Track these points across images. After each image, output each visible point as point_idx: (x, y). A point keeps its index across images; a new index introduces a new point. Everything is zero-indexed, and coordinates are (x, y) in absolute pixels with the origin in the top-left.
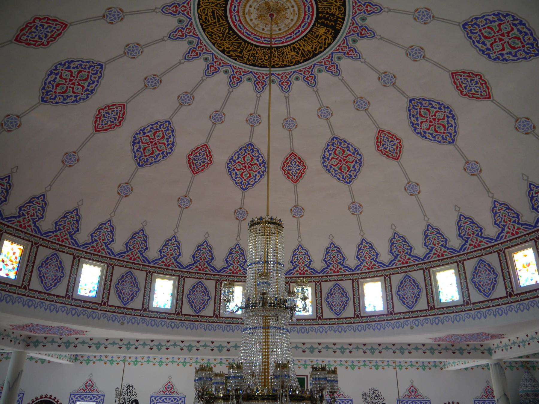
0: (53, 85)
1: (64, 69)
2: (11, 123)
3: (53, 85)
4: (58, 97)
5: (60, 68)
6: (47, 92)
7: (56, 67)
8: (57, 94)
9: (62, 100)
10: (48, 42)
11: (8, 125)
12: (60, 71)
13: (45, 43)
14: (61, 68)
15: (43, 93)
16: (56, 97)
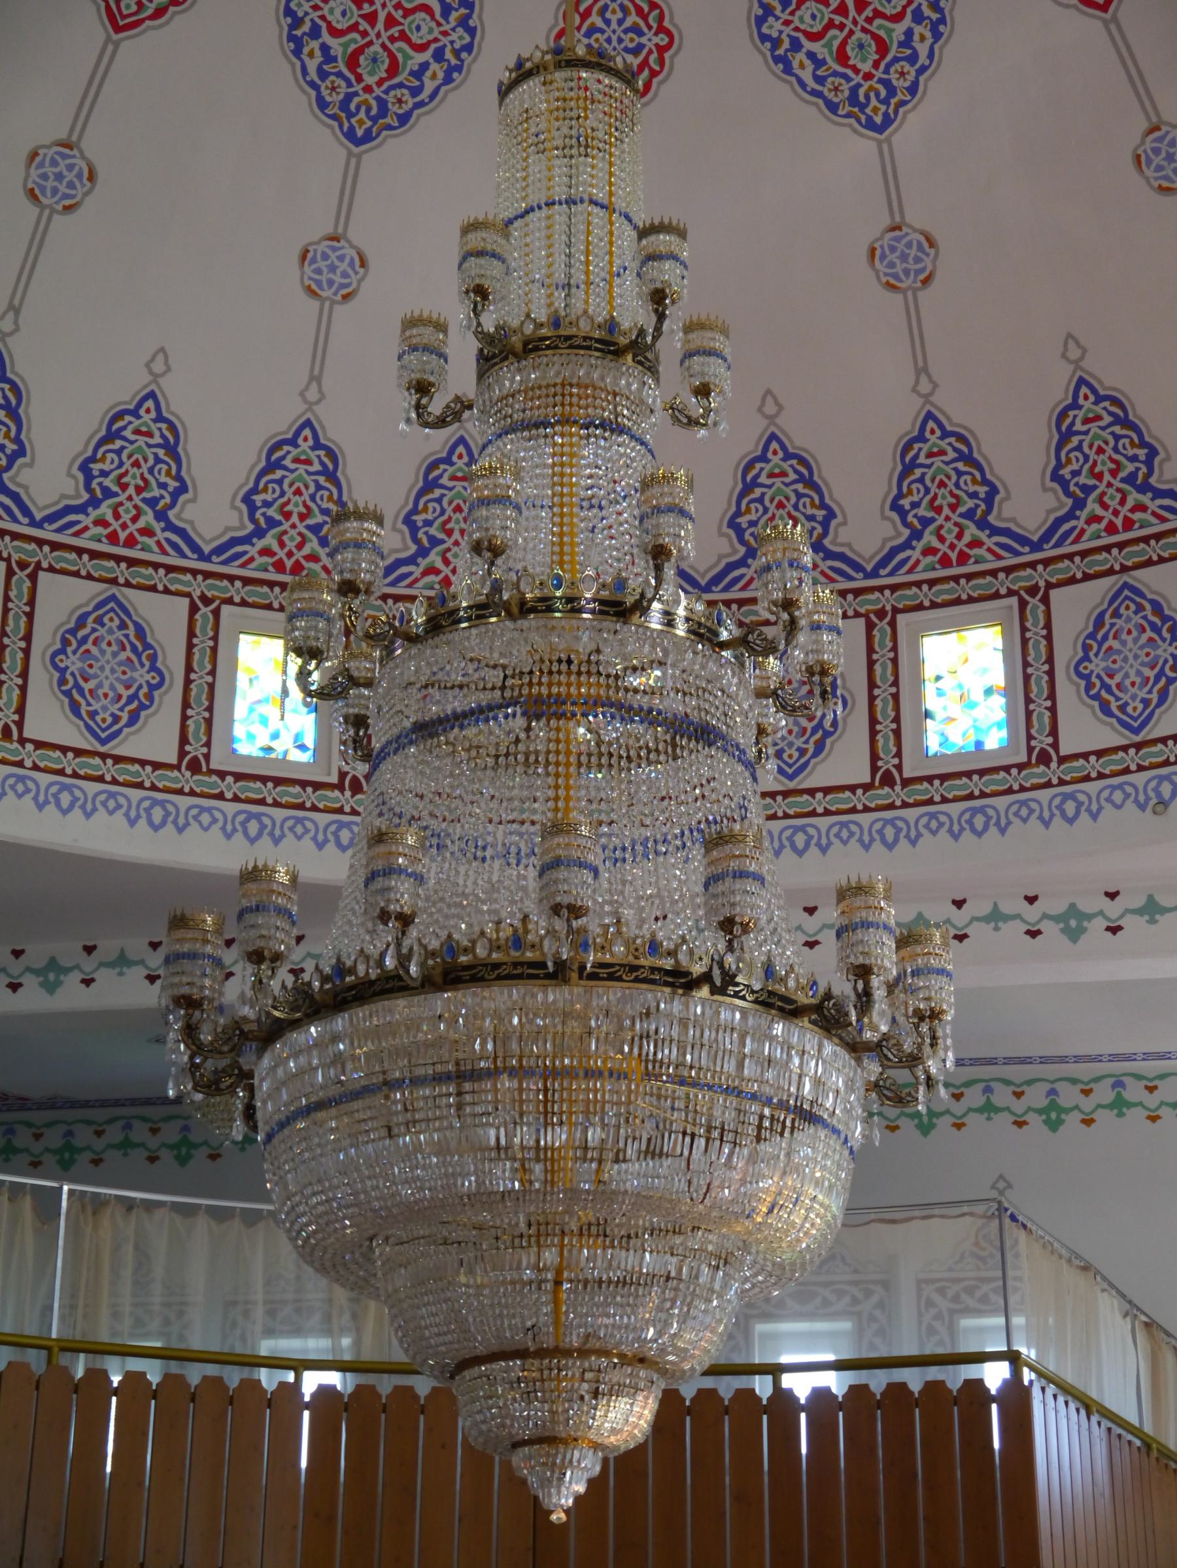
0: (835, 74)
1: (785, 16)
2: (904, 258)
3: (835, 74)
4: (893, 76)
5: (773, 27)
6: (853, 99)
7: (764, 38)
8: (879, 74)
9: (912, 72)
10: (661, 29)
11: (907, 272)
12: (788, 30)
13: (663, 40)
14: (778, 25)
15: (849, 115)
16: (886, 83)
